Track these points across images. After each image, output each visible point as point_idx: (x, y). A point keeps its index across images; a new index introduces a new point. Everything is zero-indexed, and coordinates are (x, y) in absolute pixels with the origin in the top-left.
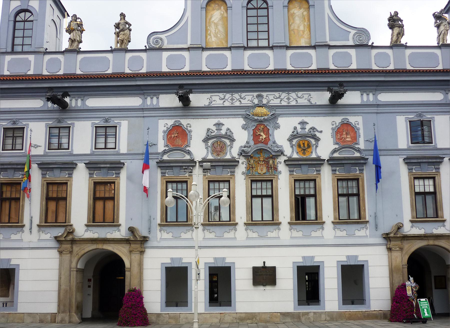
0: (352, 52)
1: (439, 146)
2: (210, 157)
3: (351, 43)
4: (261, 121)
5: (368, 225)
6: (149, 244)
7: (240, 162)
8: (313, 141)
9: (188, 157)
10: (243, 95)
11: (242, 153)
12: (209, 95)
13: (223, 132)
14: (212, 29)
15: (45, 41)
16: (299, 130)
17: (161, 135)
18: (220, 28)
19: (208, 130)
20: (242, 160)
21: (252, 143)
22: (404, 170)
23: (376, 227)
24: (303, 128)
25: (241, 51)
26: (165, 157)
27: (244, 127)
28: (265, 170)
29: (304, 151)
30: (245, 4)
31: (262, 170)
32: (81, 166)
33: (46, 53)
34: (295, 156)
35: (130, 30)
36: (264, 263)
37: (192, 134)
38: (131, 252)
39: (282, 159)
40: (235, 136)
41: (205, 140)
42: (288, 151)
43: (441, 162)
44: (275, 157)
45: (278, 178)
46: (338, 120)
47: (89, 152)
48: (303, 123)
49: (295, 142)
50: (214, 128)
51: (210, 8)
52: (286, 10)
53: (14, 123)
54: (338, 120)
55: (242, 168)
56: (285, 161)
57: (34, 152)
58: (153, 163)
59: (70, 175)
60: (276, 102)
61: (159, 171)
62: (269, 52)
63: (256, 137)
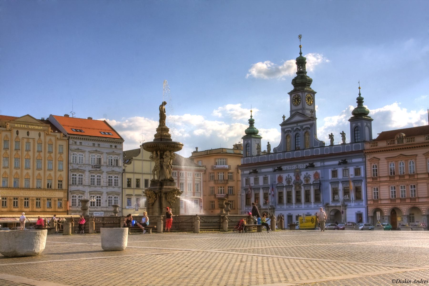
0: (319, 149)
1: (339, 178)
2: (287, 185)
3: (319, 146)
4: (298, 173)
5: (322, 203)
6: (275, 210)
7: (293, 186)
8: (309, 178)
9: (282, 185)
10: (294, 166)
11: (293, 183)
12: (286, 166)
13: (290, 177)
14: (288, 145)
15: (252, 152)
16: (306, 175)
17: (277, 179)
18: (290, 144)
19: (286, 177)
20: (294, 185)
21: (296, 180)
22: (330, 186)
23: (323, 203)
24: (307, 175)
25: (293, 152)
26: (278, 185)
27: (294, 175)
28: (298, 188)
29: (307, 182)
30: (294, 136)
31: (298, 188)
32: (261, 189)
33: (253, 156)
34: (305, 183)
35: (270, 147)
36: (298, 214)
37: (283, 178)
38: (271, 212)
39: (302, 184)
40: (292, 178)
41: (286, 180)
42: (304, 182)
43: (339, 183)
44: (300, 184)
45: (301, 190)
46: (315, 171)
47: (262, 185)
48: (307, 173)
49: (305, 179)
50: (287, 176)
51: (287, 138)
52: (304, 137)
53: (247, 178)
54: (315, 171)
55: (294, 188)
56: (302, 185)
57: (251, 185)
58: (274, 187)
59: (259, 191)
60: (301, 167)
61: (277, 189)
62: (300, 151)
63: (296, 178)
